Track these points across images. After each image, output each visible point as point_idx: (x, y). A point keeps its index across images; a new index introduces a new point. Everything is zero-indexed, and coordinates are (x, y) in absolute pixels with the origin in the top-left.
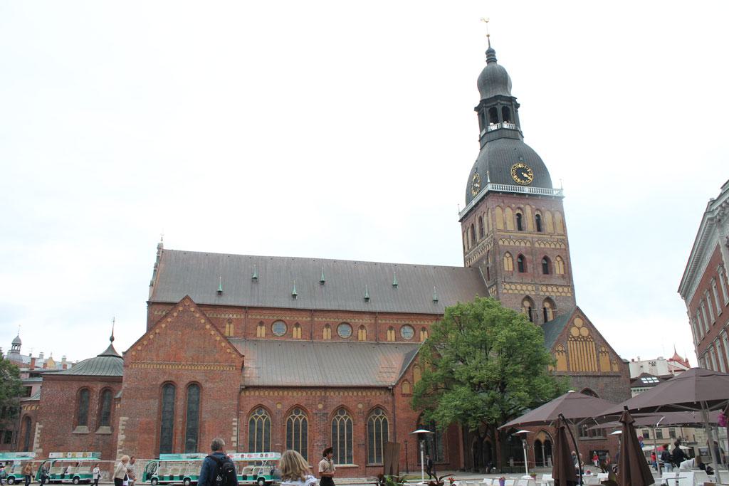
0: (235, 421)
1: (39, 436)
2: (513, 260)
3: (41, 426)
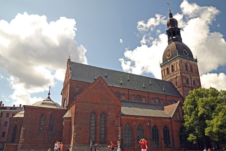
0: (120, 129)
1: (23, 133)
2: (186, 79)
3: (24, 129)
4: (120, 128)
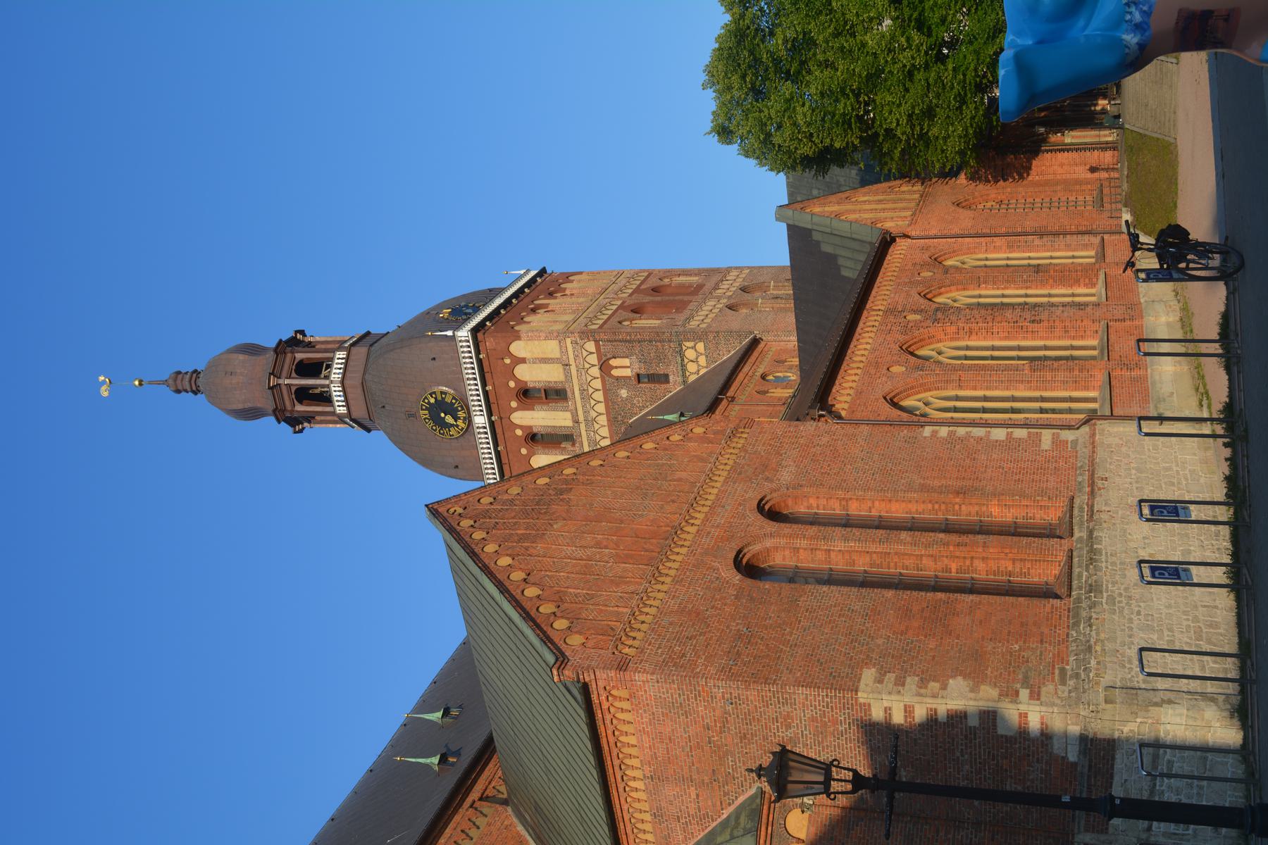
4: (927, 431)
